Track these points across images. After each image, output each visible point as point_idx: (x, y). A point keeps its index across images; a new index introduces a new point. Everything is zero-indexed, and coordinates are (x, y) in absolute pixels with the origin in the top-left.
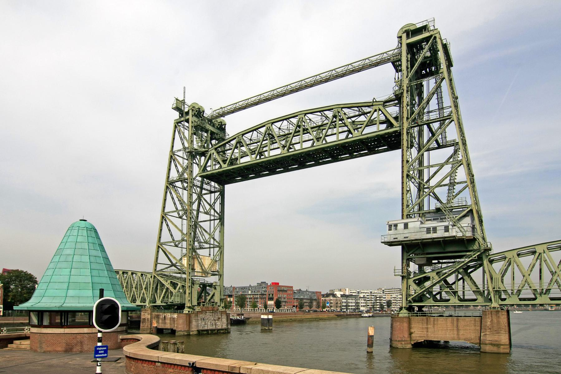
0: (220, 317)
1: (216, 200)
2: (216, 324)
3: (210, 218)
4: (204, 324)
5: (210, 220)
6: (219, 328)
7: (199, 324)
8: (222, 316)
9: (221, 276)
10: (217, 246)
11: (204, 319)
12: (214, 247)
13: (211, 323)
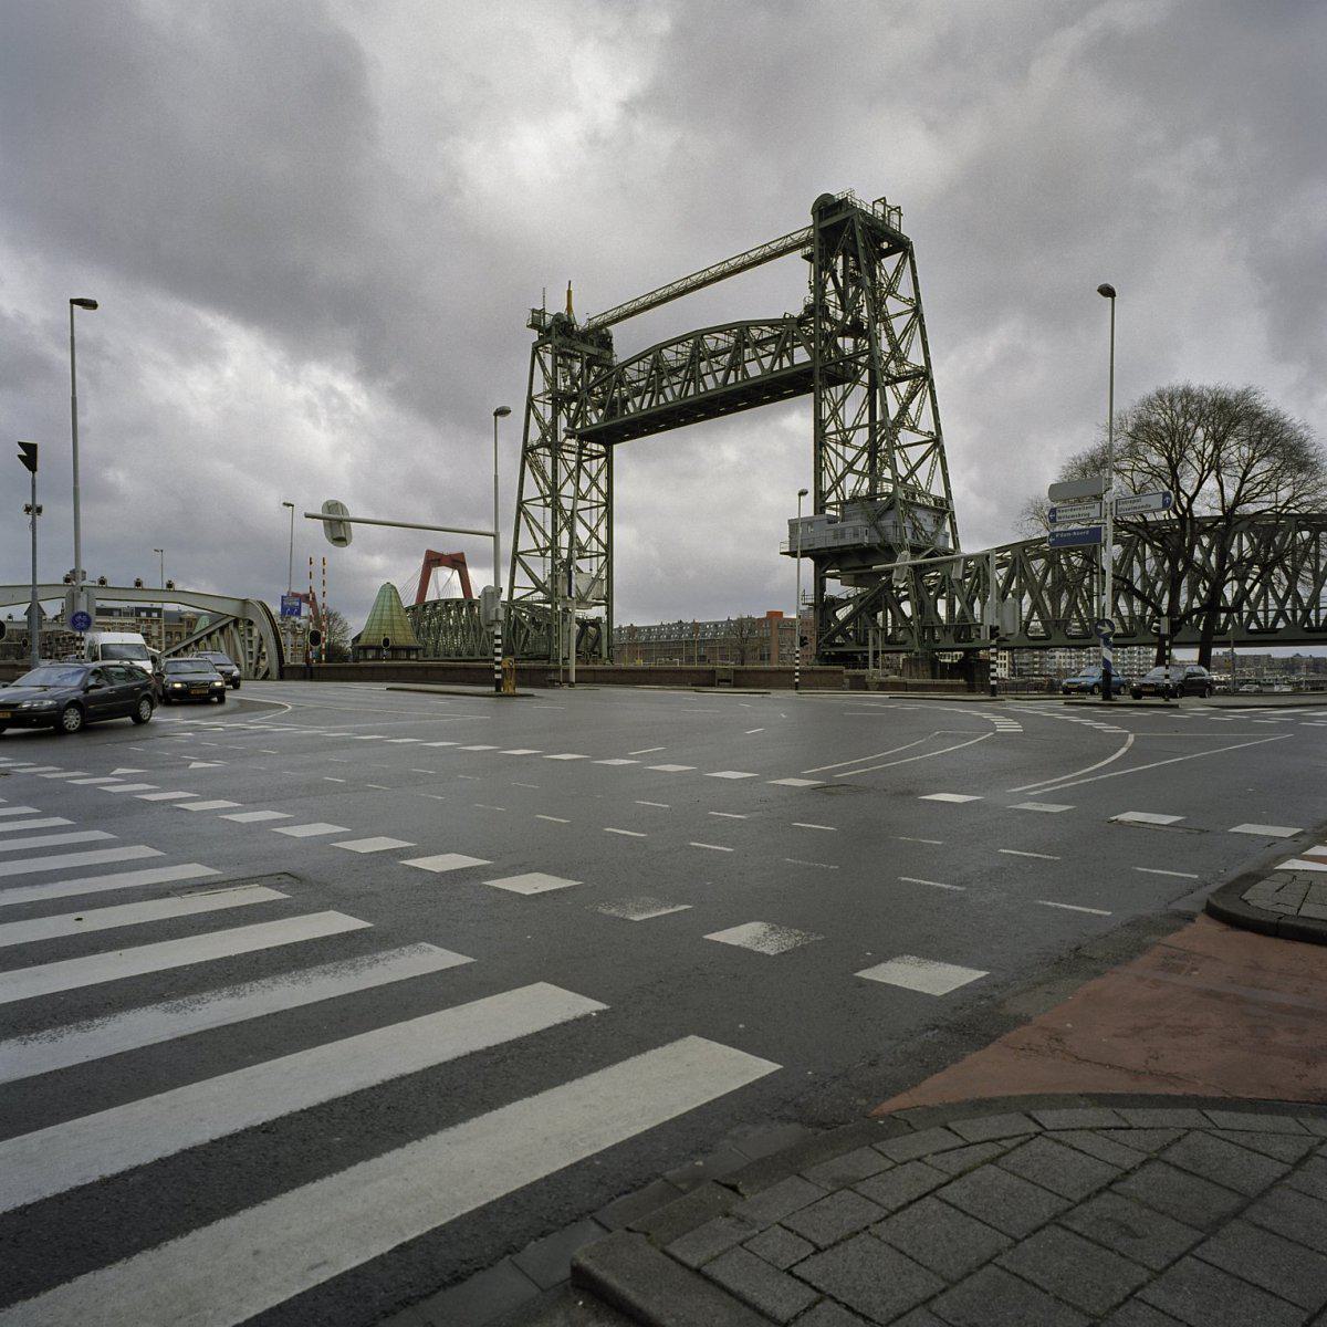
1: (600, 470)
5: (591, 508)
9: (608, 601)
10: (602, 554)
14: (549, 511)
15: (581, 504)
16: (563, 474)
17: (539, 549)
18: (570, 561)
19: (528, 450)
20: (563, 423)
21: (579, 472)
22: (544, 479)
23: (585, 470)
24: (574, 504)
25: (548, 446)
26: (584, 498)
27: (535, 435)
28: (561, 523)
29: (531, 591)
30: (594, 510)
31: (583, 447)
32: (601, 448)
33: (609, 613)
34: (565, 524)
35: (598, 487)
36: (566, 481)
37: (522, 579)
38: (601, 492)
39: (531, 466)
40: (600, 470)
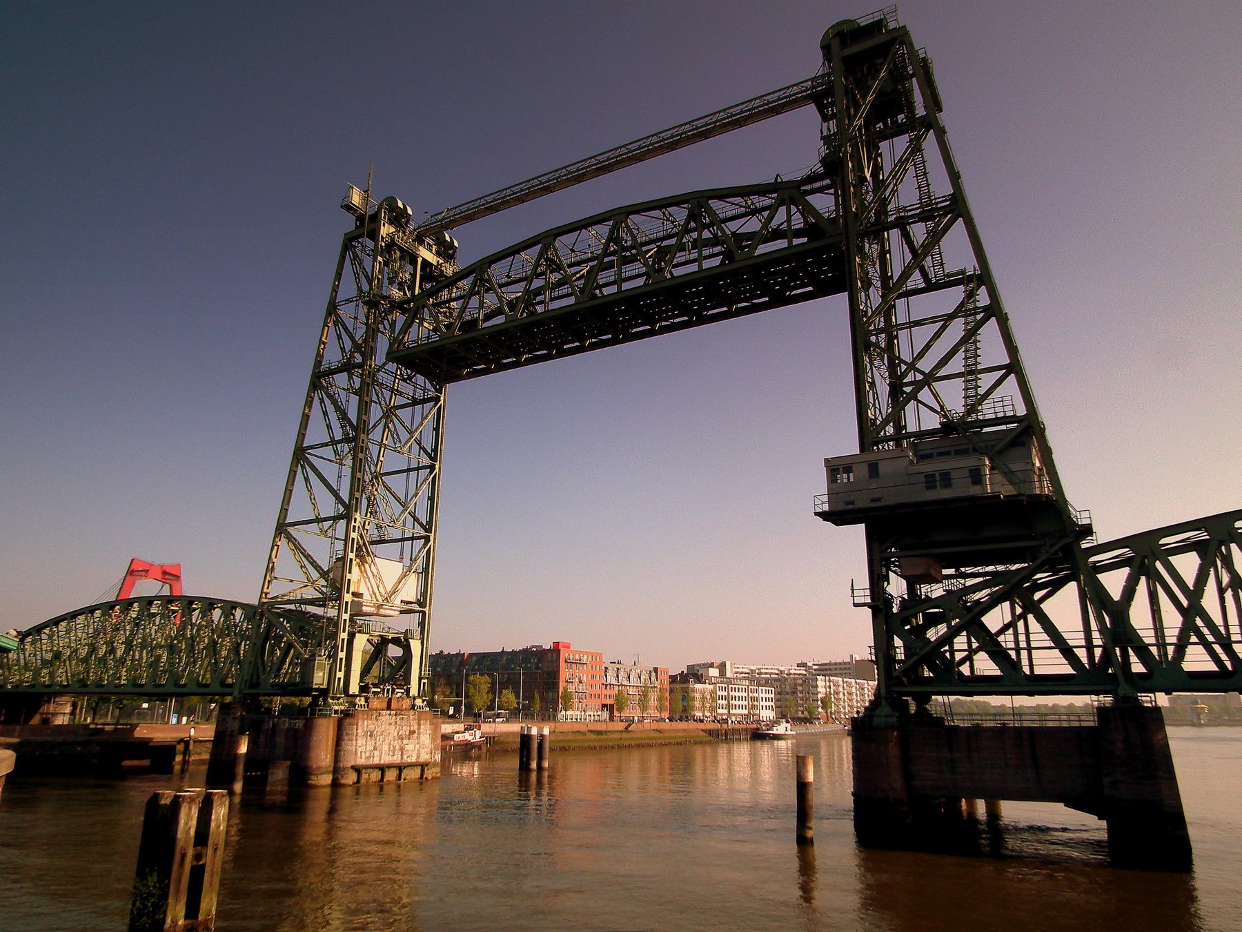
0: (416, 728)
2: (402, 749)
6: (409, 760)
8: (419, 725)
13: (390, 744)
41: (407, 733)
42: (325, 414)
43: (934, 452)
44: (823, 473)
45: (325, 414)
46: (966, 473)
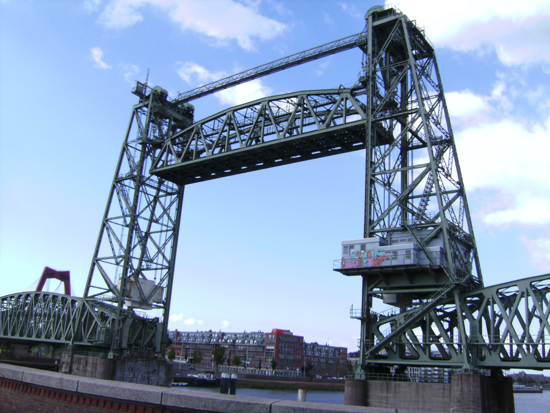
0: (157, 368)
1: (172, 203)
3: (162, 228)
4: (132, 376)
5: (161, 231)
7: (125, 376)
8: (159, 367)
9: (166, 306)
10: (166, 267)
11: (132, 370)
12: (162, 269)
13: (142, 376)
14: (127, 230)
15: (155, 227)
16: (143, 202)
17: (115, 257)
18: (139, 271)
19: (118, 180)
20: (148, 163)
21: (155, 204)
22: (127, 203)
23: (160, 203)
24: (150, 226)
25: (133, 178)
26: (157, 221)
27: (125, 170)
28: (135, 240)
29: (106, 291)
30: (164, 234)
31: (161, 183)
32: (176, 187)
33: (166, 315)
34: (139, 242)
35: (169, 217)
36: (147, 207)
37: (98, 280)
38: (171, 220)
39: (118, 194)
40: (172, 203)
41: (152, 370)
42: (120, 201)
43: (399, 239)
44: (340, 249)
45: (120, 201)
46: (404, 252)
